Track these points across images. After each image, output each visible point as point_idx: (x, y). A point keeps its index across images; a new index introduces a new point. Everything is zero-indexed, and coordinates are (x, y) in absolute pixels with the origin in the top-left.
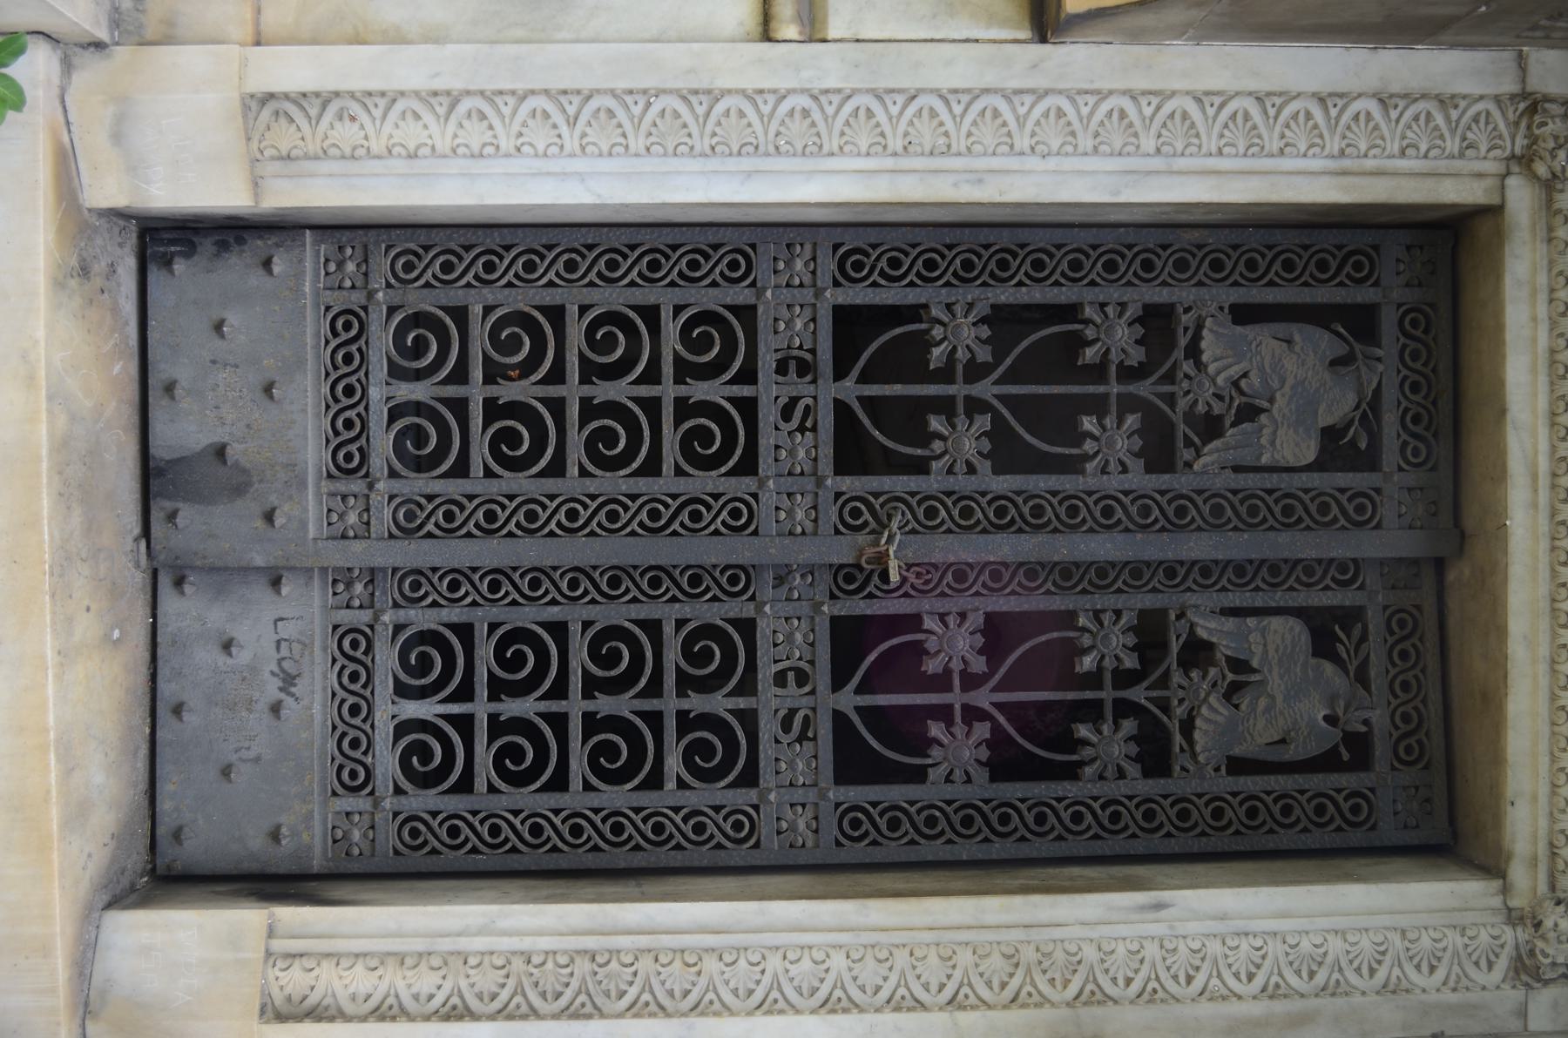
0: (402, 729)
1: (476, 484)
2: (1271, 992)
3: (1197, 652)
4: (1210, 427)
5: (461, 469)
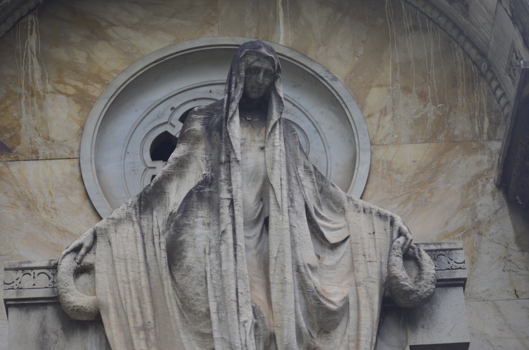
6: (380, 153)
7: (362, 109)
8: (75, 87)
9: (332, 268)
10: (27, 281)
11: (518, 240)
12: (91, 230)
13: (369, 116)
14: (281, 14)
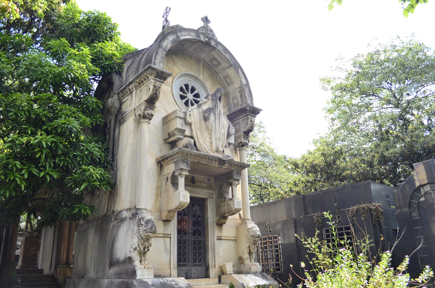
2: (213, 212)
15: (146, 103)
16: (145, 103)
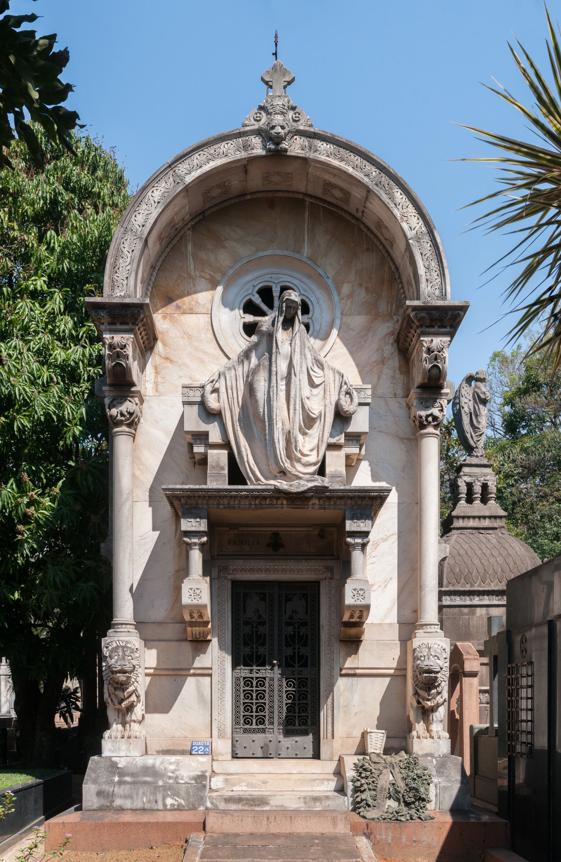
0: (300, 725)
1: (267, 714)
3: (291, 617)
4: (260, 616)
5: (265, 716)
6: (345, 319)
7: (339, 295)
8: (210, 274)
9: (316, 395)
10: (191, 393)
11: (400, 369)
12: (218, 372)
13: (342, 299)
14: (306, 238)
15: (112, 389)
16: (110, 391)
